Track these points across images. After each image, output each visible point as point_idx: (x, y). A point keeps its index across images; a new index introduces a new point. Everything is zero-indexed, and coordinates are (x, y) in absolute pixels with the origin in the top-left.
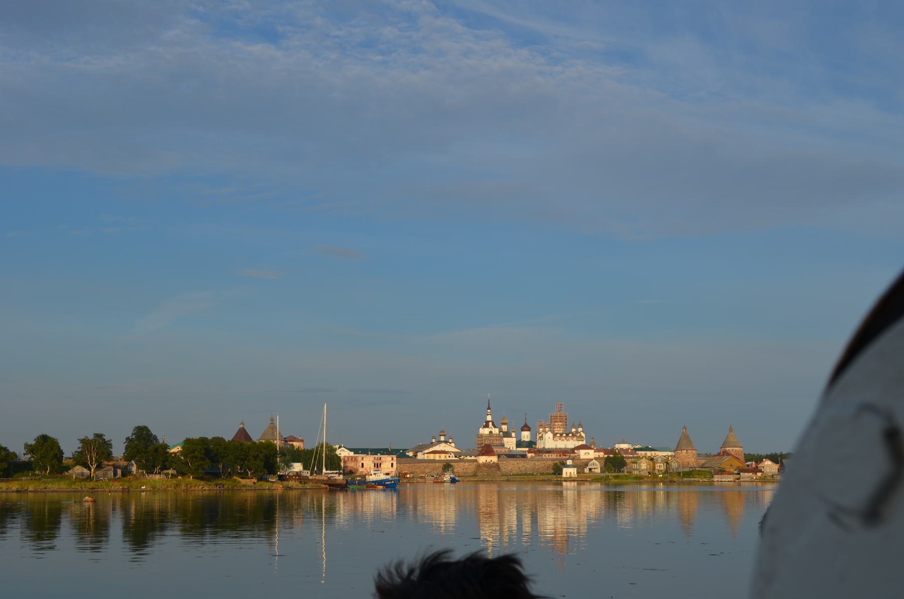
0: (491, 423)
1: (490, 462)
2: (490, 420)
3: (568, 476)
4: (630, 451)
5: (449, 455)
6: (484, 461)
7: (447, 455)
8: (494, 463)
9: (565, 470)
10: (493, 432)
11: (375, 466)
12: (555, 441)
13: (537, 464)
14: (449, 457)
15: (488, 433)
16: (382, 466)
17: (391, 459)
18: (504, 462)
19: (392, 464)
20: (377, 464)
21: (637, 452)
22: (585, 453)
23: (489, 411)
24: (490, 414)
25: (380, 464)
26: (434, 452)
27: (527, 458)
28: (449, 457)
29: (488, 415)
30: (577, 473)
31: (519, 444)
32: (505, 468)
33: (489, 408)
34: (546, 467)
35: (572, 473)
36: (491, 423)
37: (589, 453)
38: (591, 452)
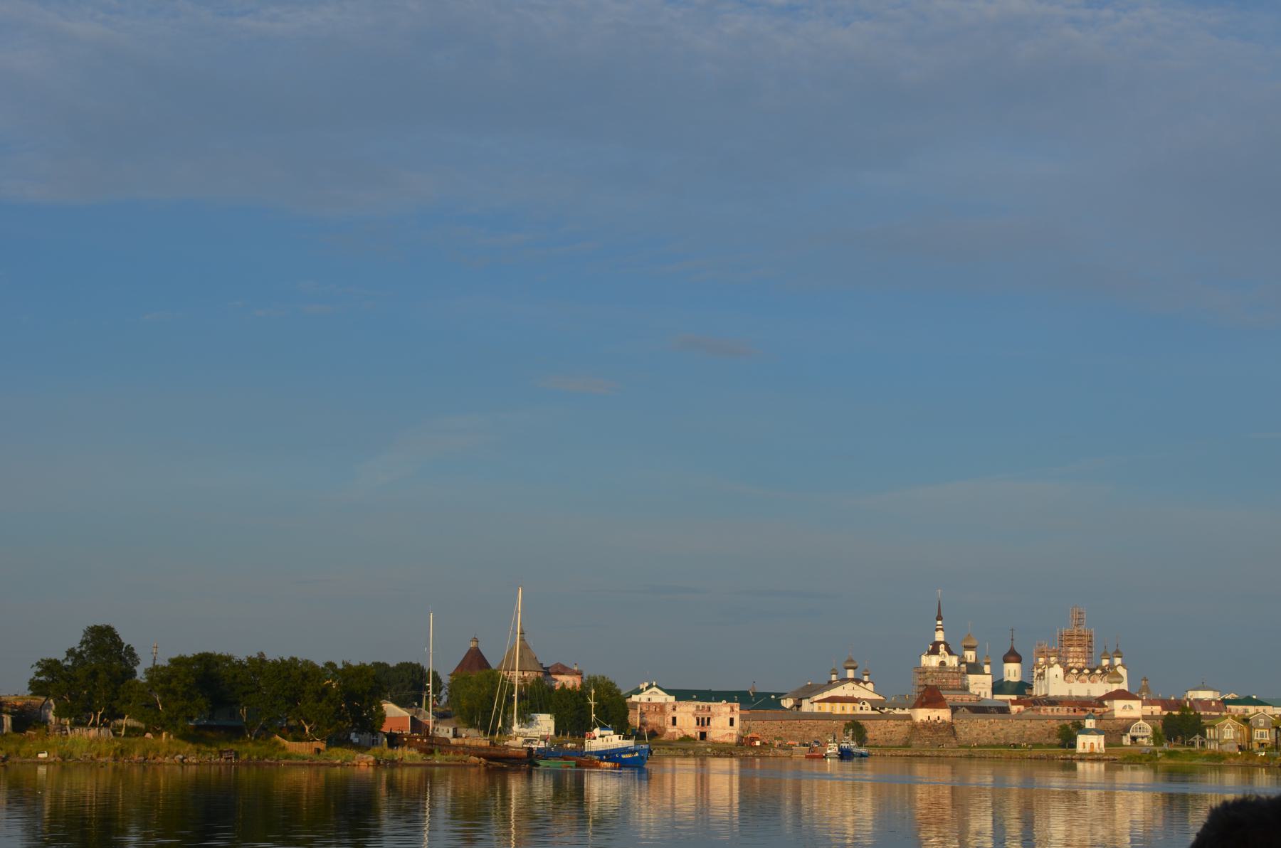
0: (942, 646)
1: (935, 721)
2: (942, 640)
3: (1087, 750)
4: (1213, 704)
6: (925, 719)
7: (858, 706)
8: (944, 722)
9: (1081, 739)
10: (948, 664)
11: (698, 724)
12: (1069, 682)
13: (1028, 726)
14: (861, 708)
15: (938, 665)
16: (711, 722)
17: (728, 709)
18: (965, 721)
19: (732, 720)
20: (703, 719)
21: (1228, 706)
22: (1124, 707)
23: (939, 622)
24: (942, 629)
25: (709, 719)
26: (832, 700)
27: (1010, 713)
28: (861, 708)
29: (937, 630)
30: (1105, 746)
31: (999, 687)
32: (966, 733)
33: (939, 618)
34: (1047, 733)
35: (1096, 746)
36: (942, 646)
37: (1131, 708)
38: (1136, 704)
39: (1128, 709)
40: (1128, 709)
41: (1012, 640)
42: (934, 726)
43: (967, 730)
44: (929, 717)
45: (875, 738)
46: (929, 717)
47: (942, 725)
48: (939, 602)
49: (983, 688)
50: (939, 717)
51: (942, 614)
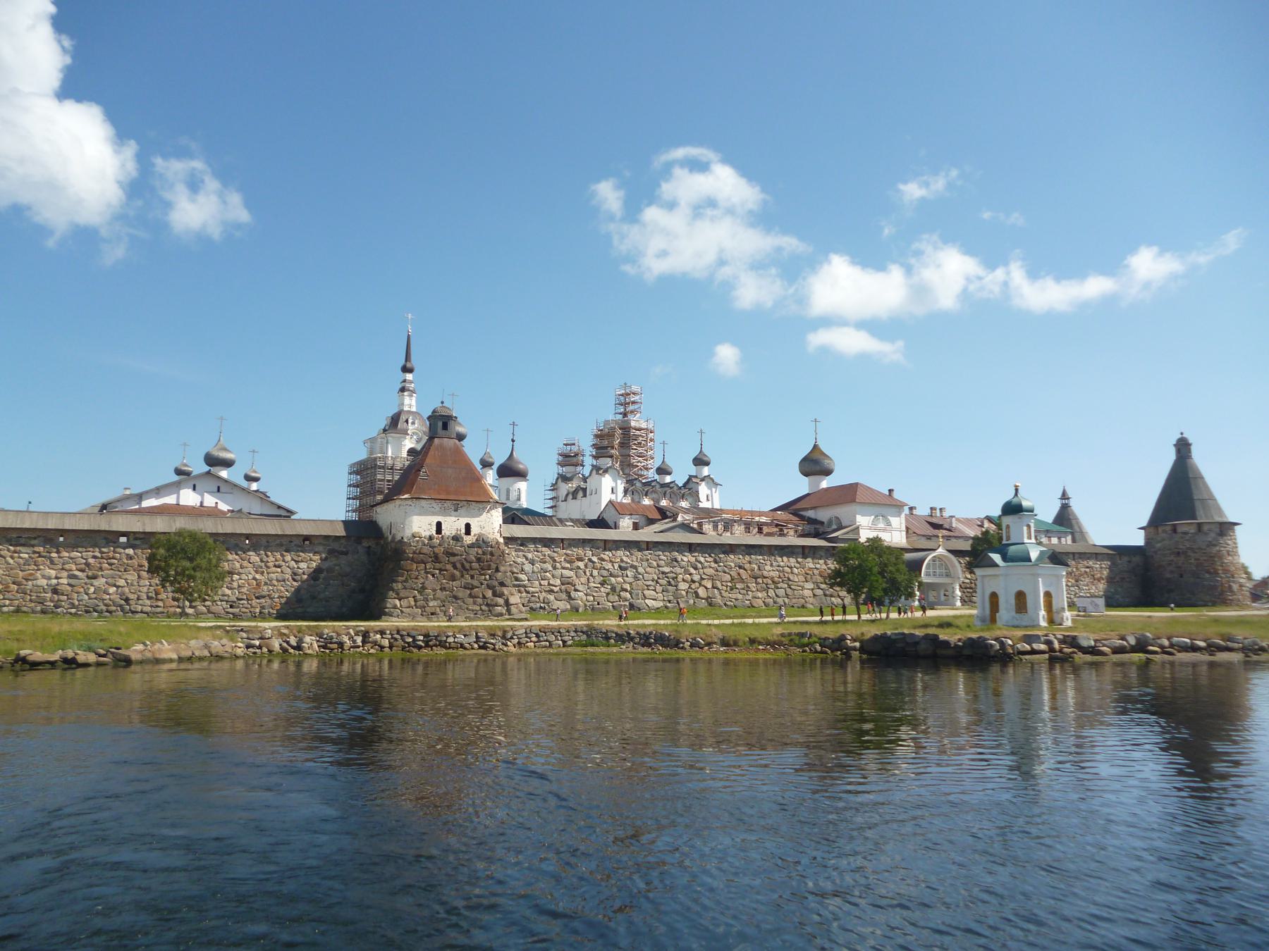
1: (456, 538)
2: (414, 409)
8: (481, 542)
23: (409, 376)
41: (513, 441)
44: (439, 525)
46: (439, 525)
50: (468, 527)
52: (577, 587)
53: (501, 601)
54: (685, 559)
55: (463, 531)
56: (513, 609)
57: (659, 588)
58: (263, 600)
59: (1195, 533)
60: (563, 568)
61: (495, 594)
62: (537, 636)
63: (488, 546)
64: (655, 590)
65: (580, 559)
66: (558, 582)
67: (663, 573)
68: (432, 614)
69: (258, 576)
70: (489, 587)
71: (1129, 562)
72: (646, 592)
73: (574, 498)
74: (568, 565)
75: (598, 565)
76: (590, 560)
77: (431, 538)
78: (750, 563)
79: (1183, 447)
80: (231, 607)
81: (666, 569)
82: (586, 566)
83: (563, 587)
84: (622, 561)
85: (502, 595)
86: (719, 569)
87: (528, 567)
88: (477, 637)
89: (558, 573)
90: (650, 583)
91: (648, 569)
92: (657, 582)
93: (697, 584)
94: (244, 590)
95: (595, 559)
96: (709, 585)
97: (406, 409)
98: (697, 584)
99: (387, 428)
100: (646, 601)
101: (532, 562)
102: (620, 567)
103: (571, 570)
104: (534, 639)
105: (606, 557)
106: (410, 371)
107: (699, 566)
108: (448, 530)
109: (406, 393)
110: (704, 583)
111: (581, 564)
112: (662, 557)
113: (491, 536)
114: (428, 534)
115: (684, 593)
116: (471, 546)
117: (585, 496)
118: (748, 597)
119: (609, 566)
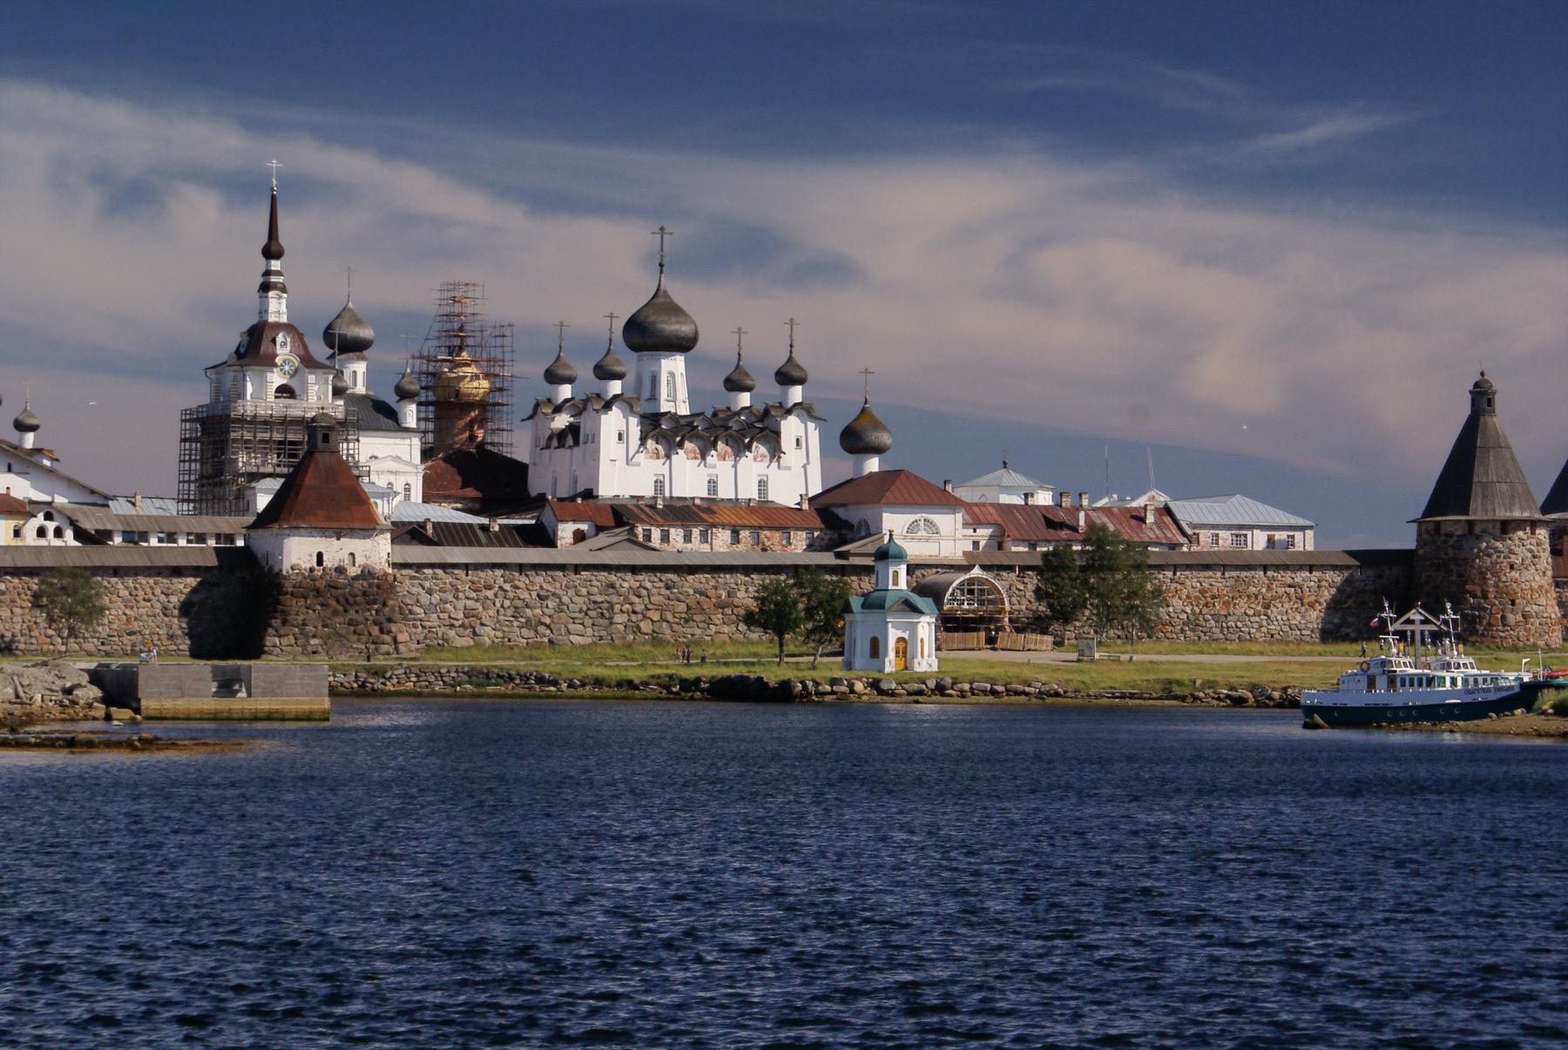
1: (340, 570)
2: (284, 319)
5: (39, 520)
8: (367, 574)
14: (41, 532)
22: (912, 528)
23: (276, 265)
34: (682, 607)
39: (922, 533)
40: (922, 533)
42: (333, 586)
43: (436, 598)
44: (320, 556)
45: (136, 626)
46: (320, 556)
47: (358, 585)
48: (273, 199)
49: (396, 473)
51: (283, 239)
52: (484, 620)
53: (387, 638)
54: (626, 585)
55: (346, 562)
56: (402, 648)
57: (588, 622)
58: (133, 637)
59: (1463, 536)
60: (468, 598)
61: (381, 631)
62: (418, 676)
63: (374, 578)
64: (583, 624)
65: (489, 587)
66: (461, 615)
67: (595, 602)
68: (314, 653)
69: (128, 612)
70: (375, 623)
71: (1380, 577)
72: (571, 627)
73: (561, 445)
74: (474, 595)
75: (511, 595)
76: (501, 588)
77: (312, 570)
78: (716, 588)
79: (1482, 397)
80: (103, 644)
81: (599, 598)
82: (496, 595)
83: (466, 621)
84: (542, 588)
85: (389, 632)
86: (672, 596)
87: (424, 598)
88: (356, 677)
89: (461, 605)
90: (577, 615)
91: (576, 599)
92: (586, 614)
93: (640, 616)
94: (115, 626)
95: (507, 587)
96: (656, 617)
97: (272, 319)
98: (640, 616)
99: (242, 350)
100: (571, 637)
101: (430, 592)
102: (538, 595)
103: (477, 601)
104: (414, 679)
105: (521, 585)
106: (278, 255)
107: (644, 592)
108: (329, 562)
109: (271, 294)
110: (649, 614)
111: (490, 594)
112: (595, 583)
113: (378, 567)
114: (308, 566)
115: (621, 627)
116: (356, 578)
117: (576, 443)
118: (708, 632)
119: (525, 595)
